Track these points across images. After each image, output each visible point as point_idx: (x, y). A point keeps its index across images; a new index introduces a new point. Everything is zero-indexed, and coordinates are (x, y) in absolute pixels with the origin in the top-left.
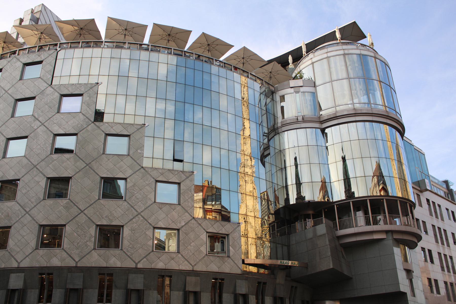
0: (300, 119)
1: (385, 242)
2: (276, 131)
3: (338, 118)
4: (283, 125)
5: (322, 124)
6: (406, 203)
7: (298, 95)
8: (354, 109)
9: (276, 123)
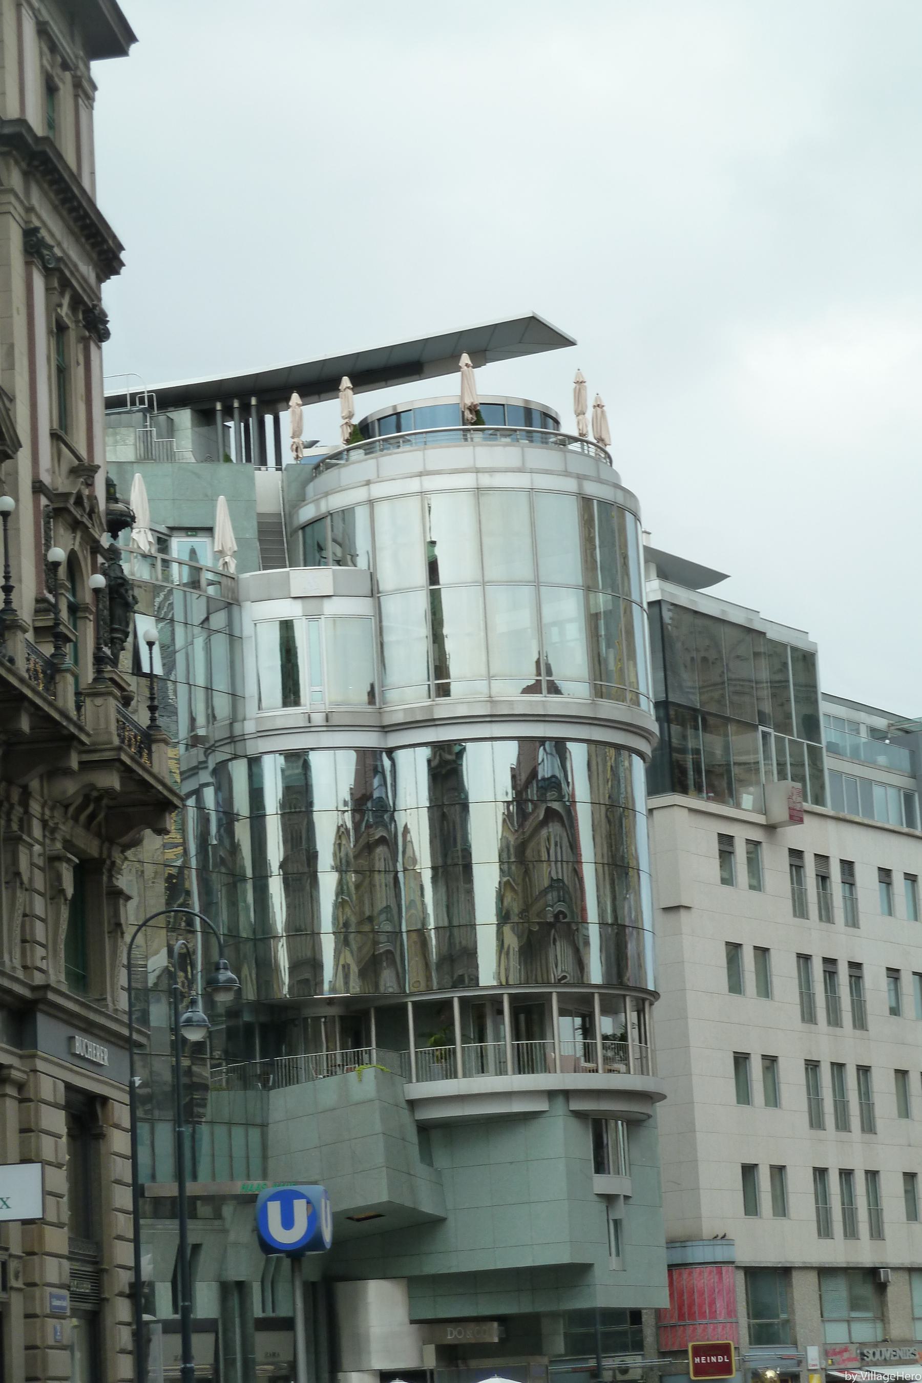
0: (318, 719)
1: (542, 1121)
2: (239, 745)
3: (437, 723)
4: (263, 734)
5: (386, 732)
6: (624, 996)
7: (313, 624)
8: (491, 701)
9: (240, 717)
